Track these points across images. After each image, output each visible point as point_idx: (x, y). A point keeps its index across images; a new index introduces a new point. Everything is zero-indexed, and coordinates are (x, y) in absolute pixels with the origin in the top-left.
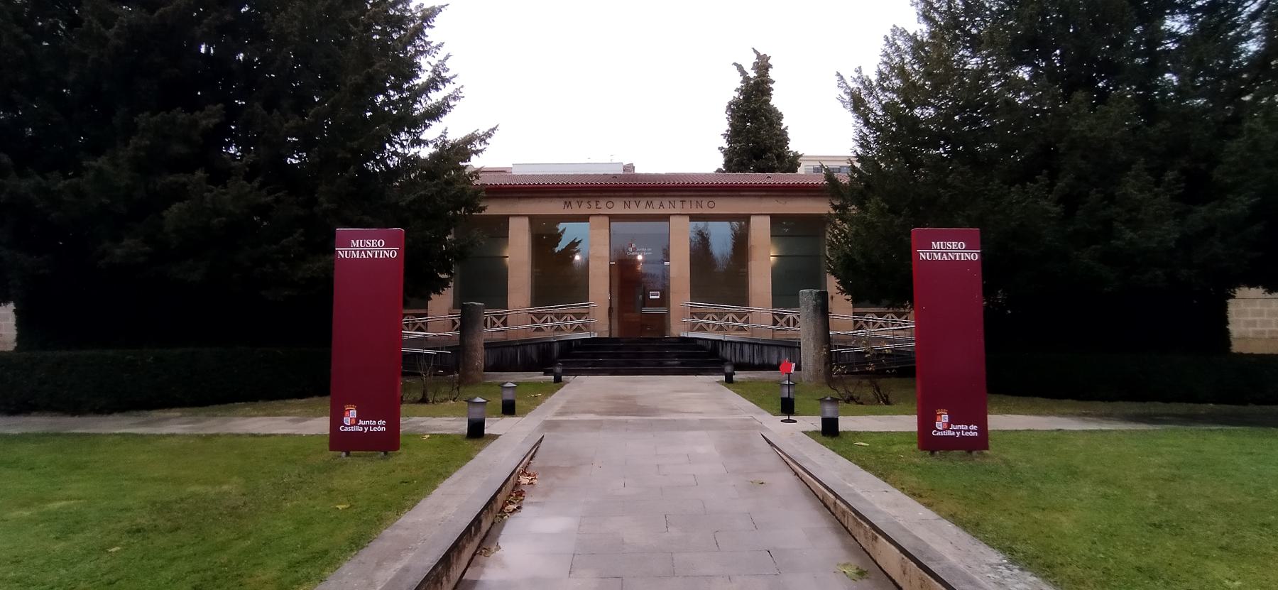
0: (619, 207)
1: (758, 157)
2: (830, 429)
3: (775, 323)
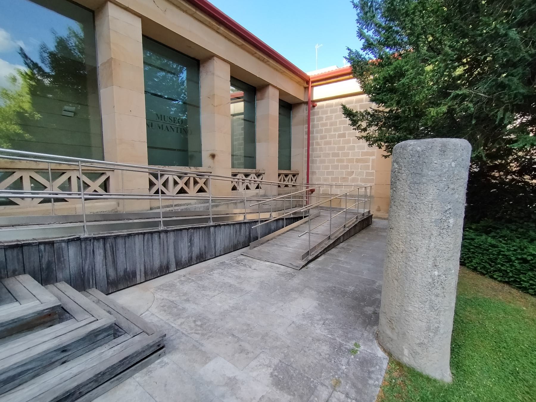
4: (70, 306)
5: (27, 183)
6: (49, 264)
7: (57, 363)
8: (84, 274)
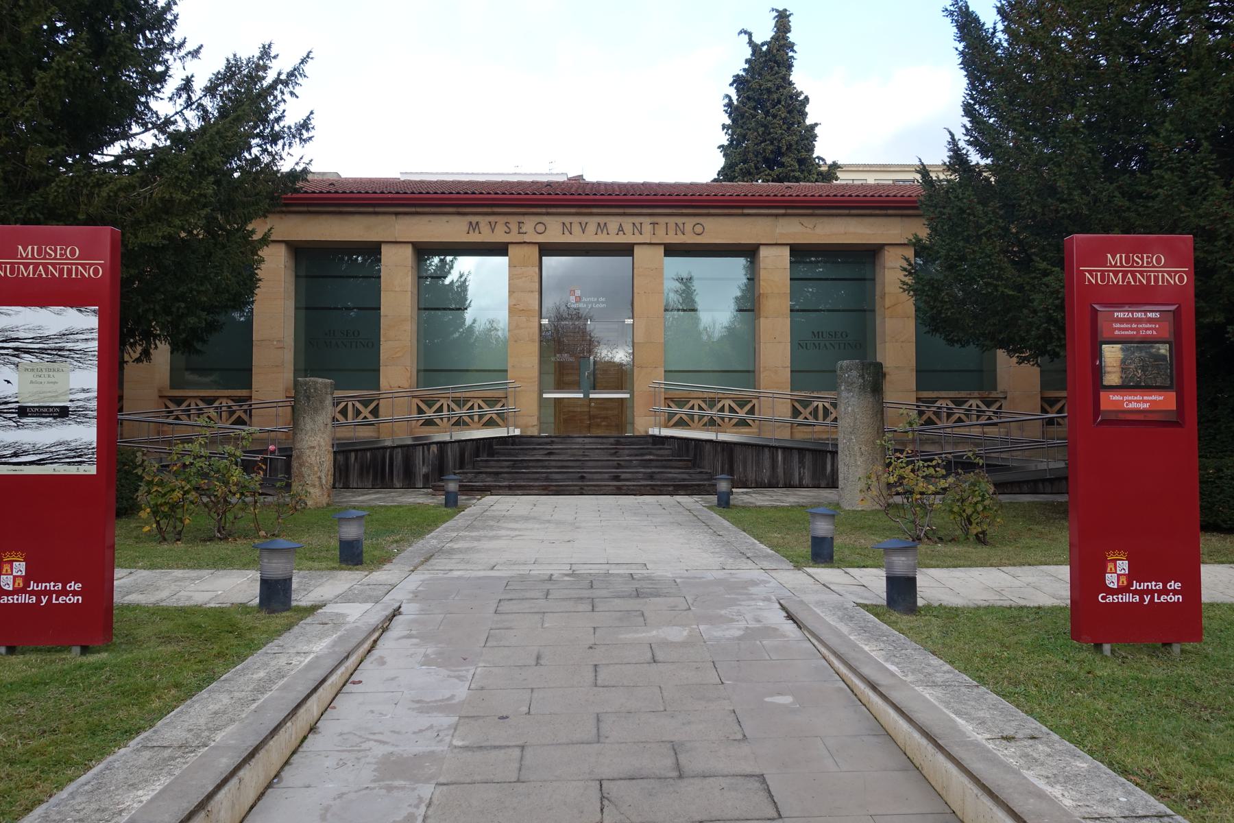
0: (554, 230)
1: (770, 163)
2: (902, 590)
3: (796, 413)
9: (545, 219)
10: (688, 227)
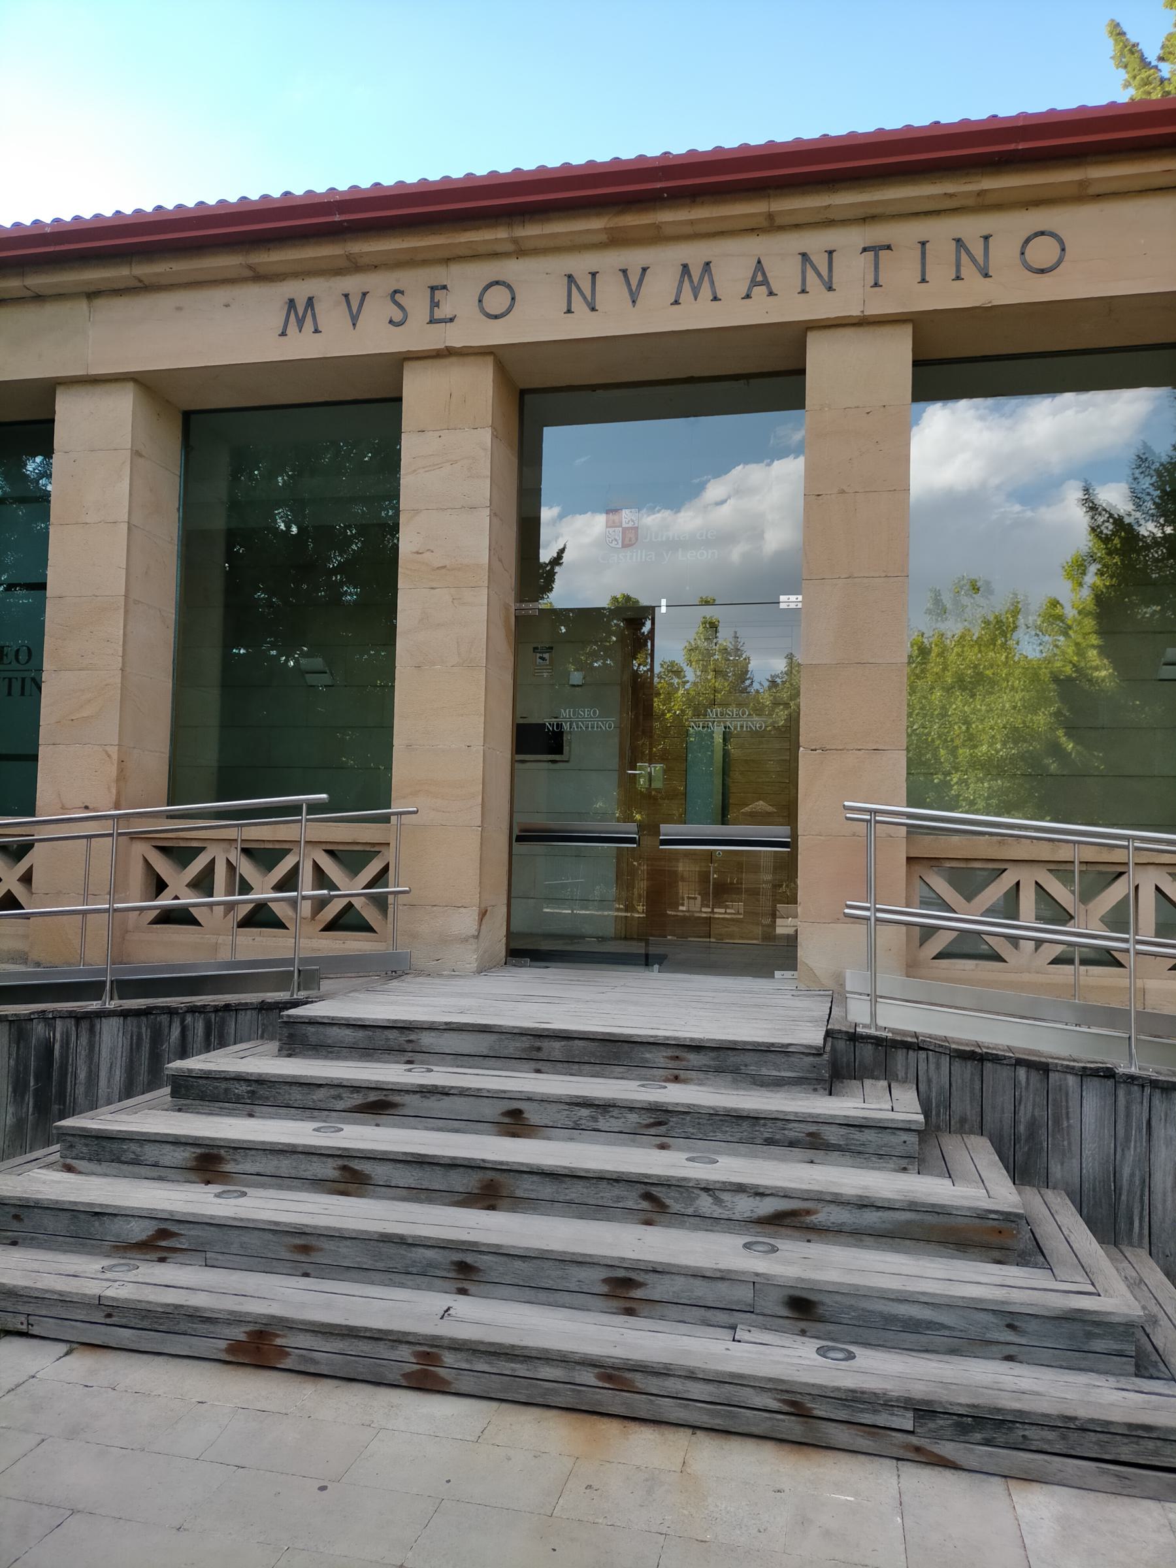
4: (1054, 1244)
5: (1028, 901)
6: (1033, 1125)
7: (994, 1348)
8: (1117, 1190)
9: (511, 269)
10: (1004, 252)
